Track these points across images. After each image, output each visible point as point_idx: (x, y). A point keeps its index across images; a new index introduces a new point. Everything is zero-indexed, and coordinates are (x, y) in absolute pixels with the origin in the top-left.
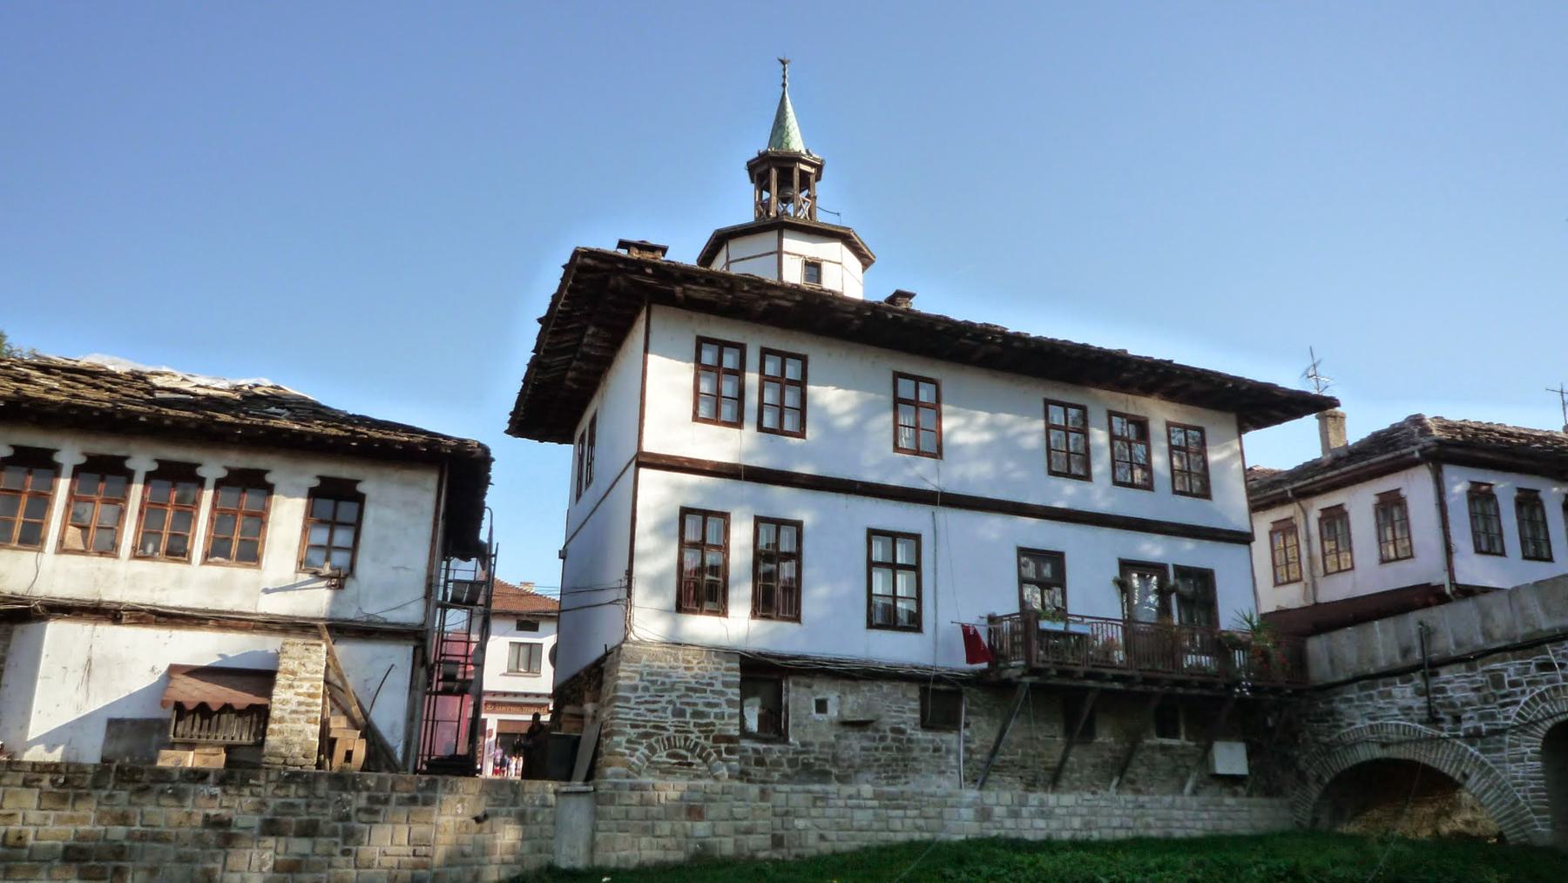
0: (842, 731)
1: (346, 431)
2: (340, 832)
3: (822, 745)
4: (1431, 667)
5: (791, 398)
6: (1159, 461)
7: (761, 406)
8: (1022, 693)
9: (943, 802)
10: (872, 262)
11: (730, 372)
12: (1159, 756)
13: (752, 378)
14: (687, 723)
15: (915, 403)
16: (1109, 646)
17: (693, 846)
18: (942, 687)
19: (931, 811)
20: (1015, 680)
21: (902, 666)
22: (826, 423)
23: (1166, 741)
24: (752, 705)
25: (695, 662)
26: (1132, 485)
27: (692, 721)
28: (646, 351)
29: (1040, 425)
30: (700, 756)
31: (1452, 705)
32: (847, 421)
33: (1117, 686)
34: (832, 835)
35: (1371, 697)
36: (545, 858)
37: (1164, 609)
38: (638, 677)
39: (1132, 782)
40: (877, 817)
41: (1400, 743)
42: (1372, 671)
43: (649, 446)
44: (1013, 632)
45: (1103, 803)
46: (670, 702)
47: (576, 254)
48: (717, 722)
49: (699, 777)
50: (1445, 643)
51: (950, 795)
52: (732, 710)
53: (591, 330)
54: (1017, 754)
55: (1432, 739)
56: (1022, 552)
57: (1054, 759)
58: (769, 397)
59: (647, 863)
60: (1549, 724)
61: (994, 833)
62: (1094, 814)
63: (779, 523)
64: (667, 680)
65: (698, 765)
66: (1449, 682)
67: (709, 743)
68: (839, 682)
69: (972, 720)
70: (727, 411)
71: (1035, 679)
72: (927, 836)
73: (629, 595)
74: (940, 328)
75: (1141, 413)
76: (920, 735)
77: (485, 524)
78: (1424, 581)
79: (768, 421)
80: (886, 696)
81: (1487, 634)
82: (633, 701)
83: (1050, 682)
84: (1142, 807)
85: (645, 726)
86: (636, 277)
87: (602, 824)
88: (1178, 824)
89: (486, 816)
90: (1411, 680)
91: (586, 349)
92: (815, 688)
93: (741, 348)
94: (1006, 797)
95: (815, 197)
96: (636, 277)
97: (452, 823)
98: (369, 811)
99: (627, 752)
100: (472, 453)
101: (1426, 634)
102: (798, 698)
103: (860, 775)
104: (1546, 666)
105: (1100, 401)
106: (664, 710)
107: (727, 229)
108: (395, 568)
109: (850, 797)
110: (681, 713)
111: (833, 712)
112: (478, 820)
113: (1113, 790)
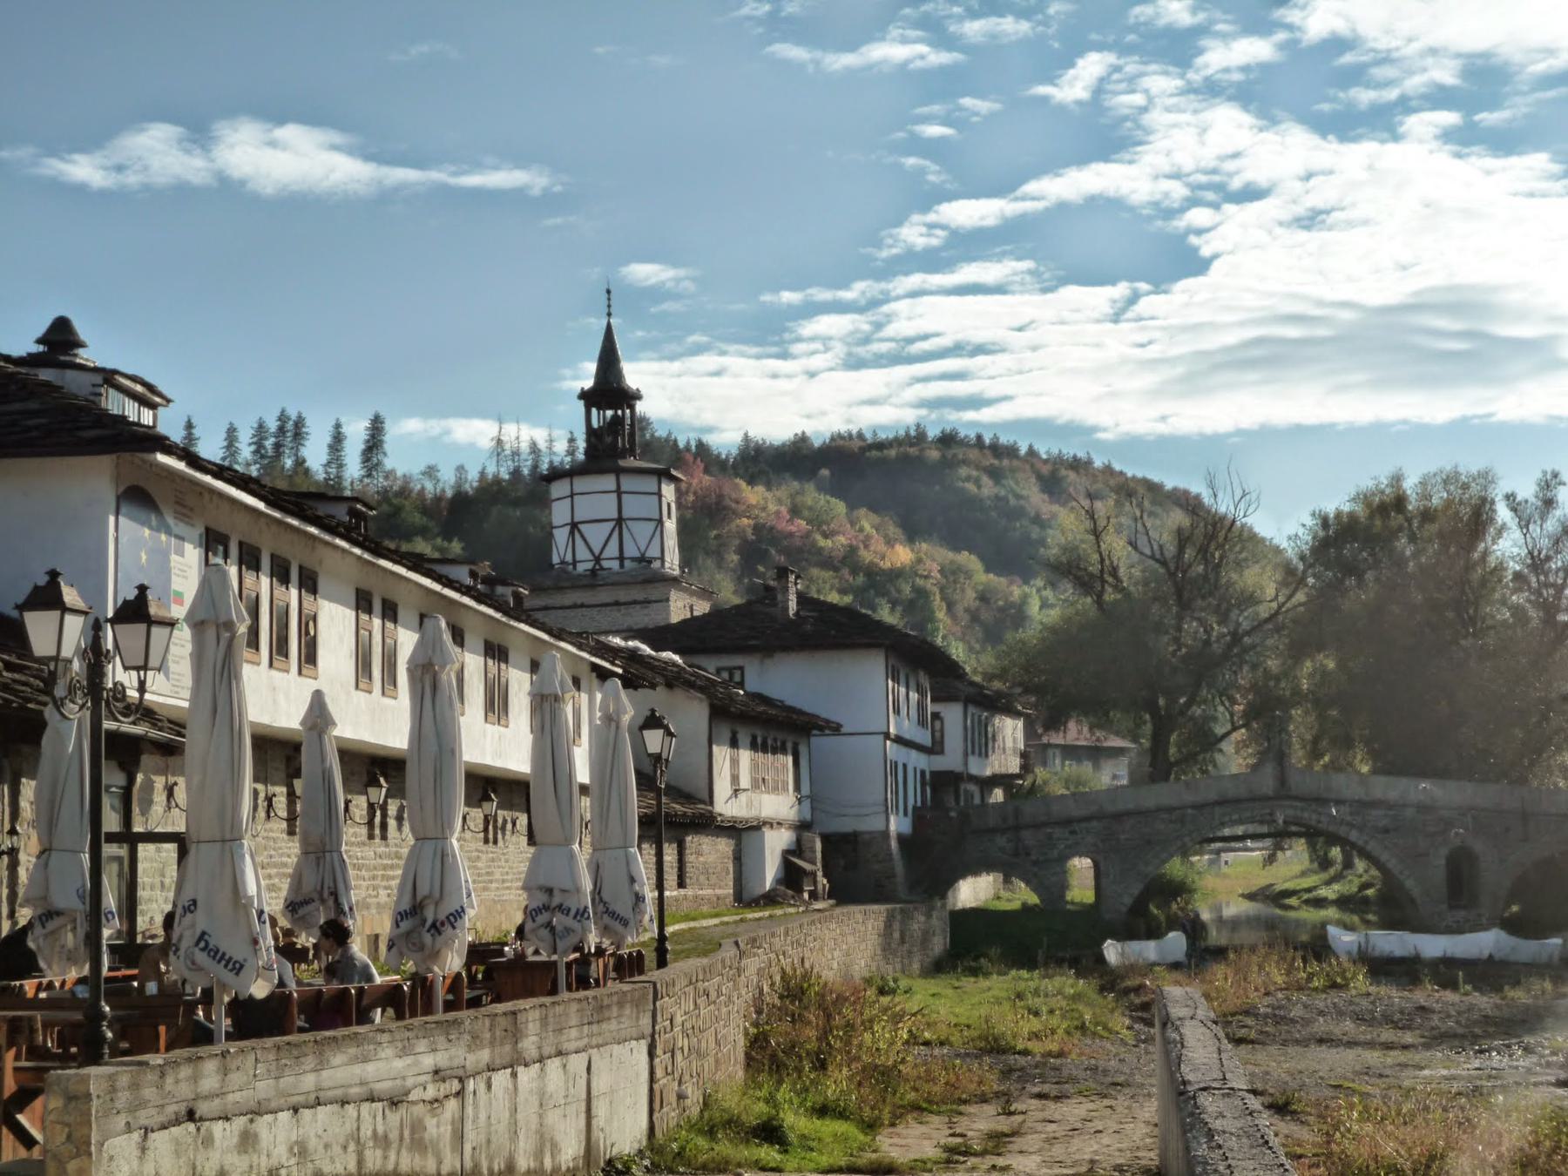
4: (1017, 828)
104: (1073, 832)
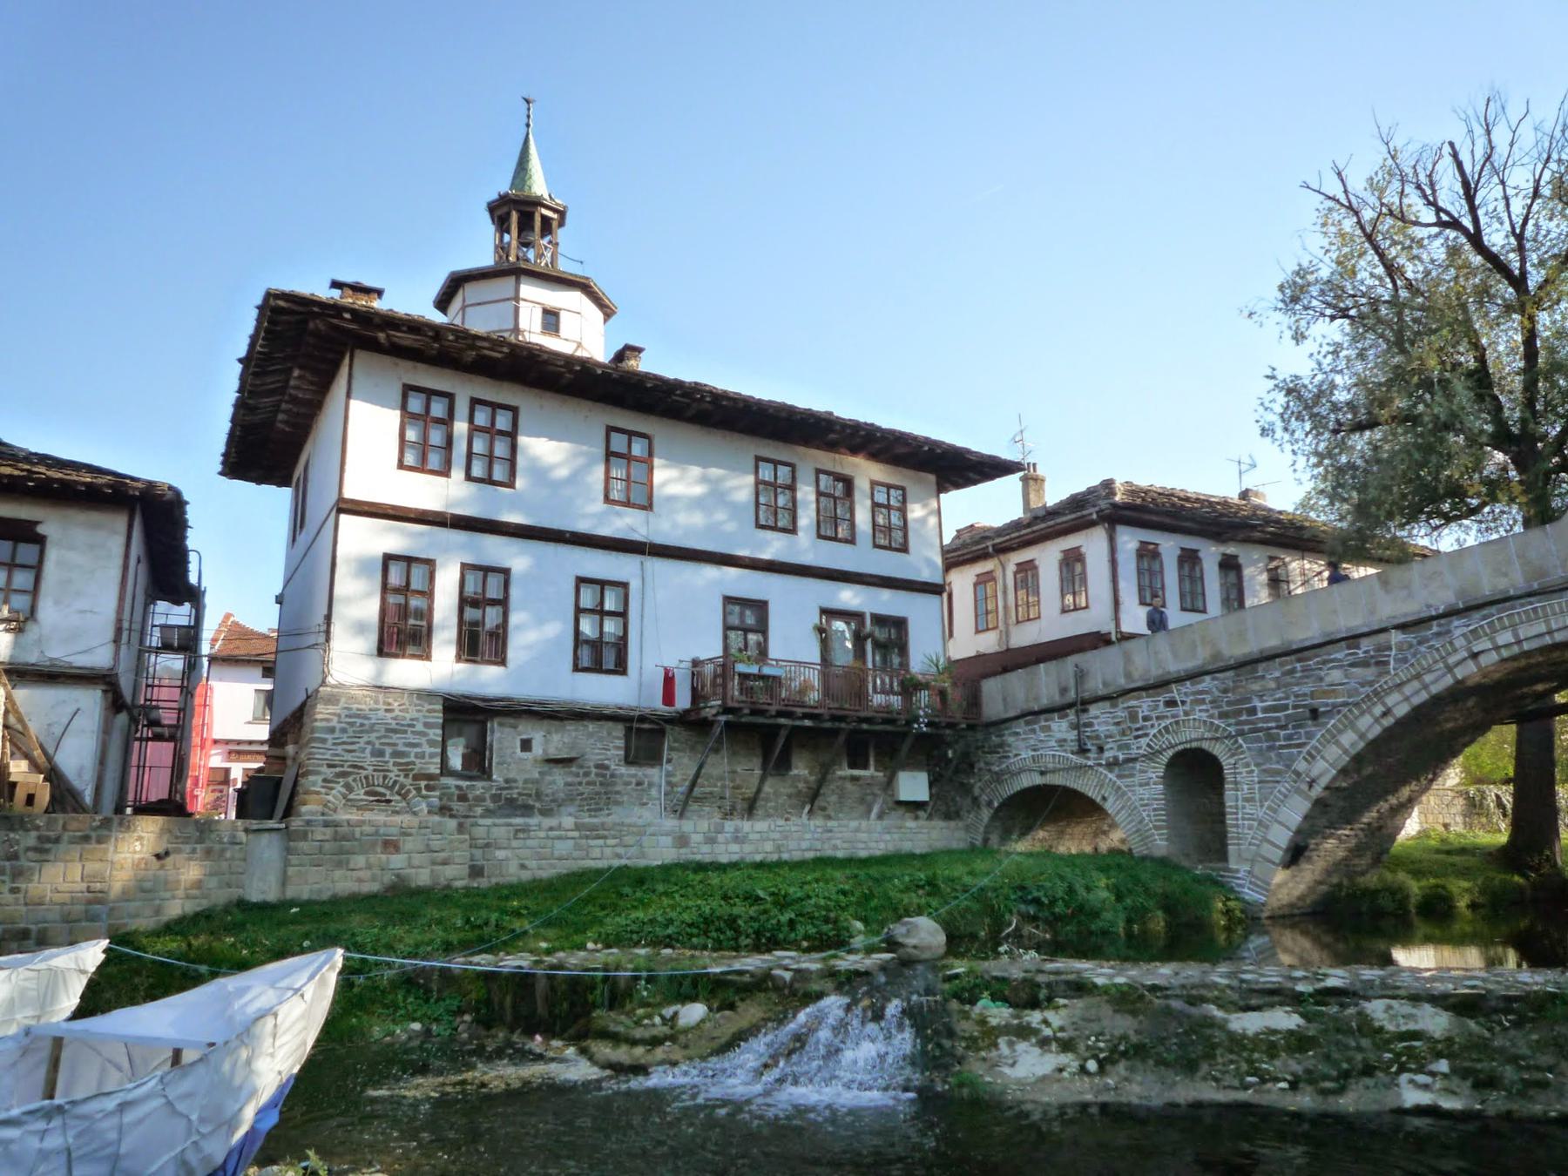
0: (546, 768)
1: (23, 470)
2: (8, 871)
3: (526, 781)
4: (1083, 704)
5: (501, 449)
6: (862, 517)
7: (470, 455)
8: (717, 730)
9: (641, 831)
10: (614, 313)
11: (439, 421)
12: (849, 786)
13: (461, 427)
14: (387, 762)
15: (627, 457)
16: (804, 689)
17: (388, 878)
18: (646, 726)
19: (629, 840)
20: (711, 718)
21: (607, 707)
22: (540, 473)
23: (856, 772)
24: (454, 745)
25: (396, 704)
26: (835, 539)
27: (392, 761)
28: (348, 396)
29: (750, 479)
30: (399, 793)
31: (1098, 737)
32: (563, 473)
33: (807, 723)
34: (532, 864)
35: (1033, 731)
36: (235, 893)
37: (859, 651)
38: (336, 719)
39: (824, 809)
40: (577, 847)
41: (1054, 771)
42: (1036, 709)
43: (349, 493)
44: (716, 676)
45: (793, 829)
46: (368, 743)
47: (269, 295)
48: (417, 761)
49: (397, 813)
50: (1095, 685)
51: (649, 825)
52: (432, 750)
53: (296, 373)
54: (716, 786)
55: (1081, 767)
56: (729, 600)
57: (749, 792)
58: (479, 446)
59: (340, 894)
60: (1170, 753)
61: (691, 857)
62: (786, 838)
63: (486, 570)
64: (366, 722)
65: (397, 802)
66: (1097, 717)
67: (409, 781)
68: (546, 722)
69: (674, 755)
70: (434, 460)
71: (730, 717)
72: (624, 862)
73: (328, 640)
74: (649, 385)
75: (847, 471)
76: (623, 770)
77: (193, 567)
78: (1095, 630)
79: (478, 470)
80: (591, 735)
81: (1128, 675)
82: (330, 742)
83: (743, 720)
84: (830, 831)
85: (342, 766)
86: (335, 321)
87: (294, 859)
88: (862, 846)
89: (167, 854)
90: (1067, 716)
91: (292, 392)
92: (520, 728)
93: (450, 397)
94: (704, 825)
95: (557, 244)
96: (335, 321)
97: (130, 861)
98: (36, 849)
99: (323, 790)
100: (164, 495)
101: (1081, 676)
102: (503, 738)
103: (562, 809)
104: (1171, 703)
105: (810, 459)
106: (363, 750)
107: (463, 271)
108: (83, 612)
109: (551, 829)
110: (381, 753)
111: (538, 749)
112: (158, 856)
113: (805, 816)
